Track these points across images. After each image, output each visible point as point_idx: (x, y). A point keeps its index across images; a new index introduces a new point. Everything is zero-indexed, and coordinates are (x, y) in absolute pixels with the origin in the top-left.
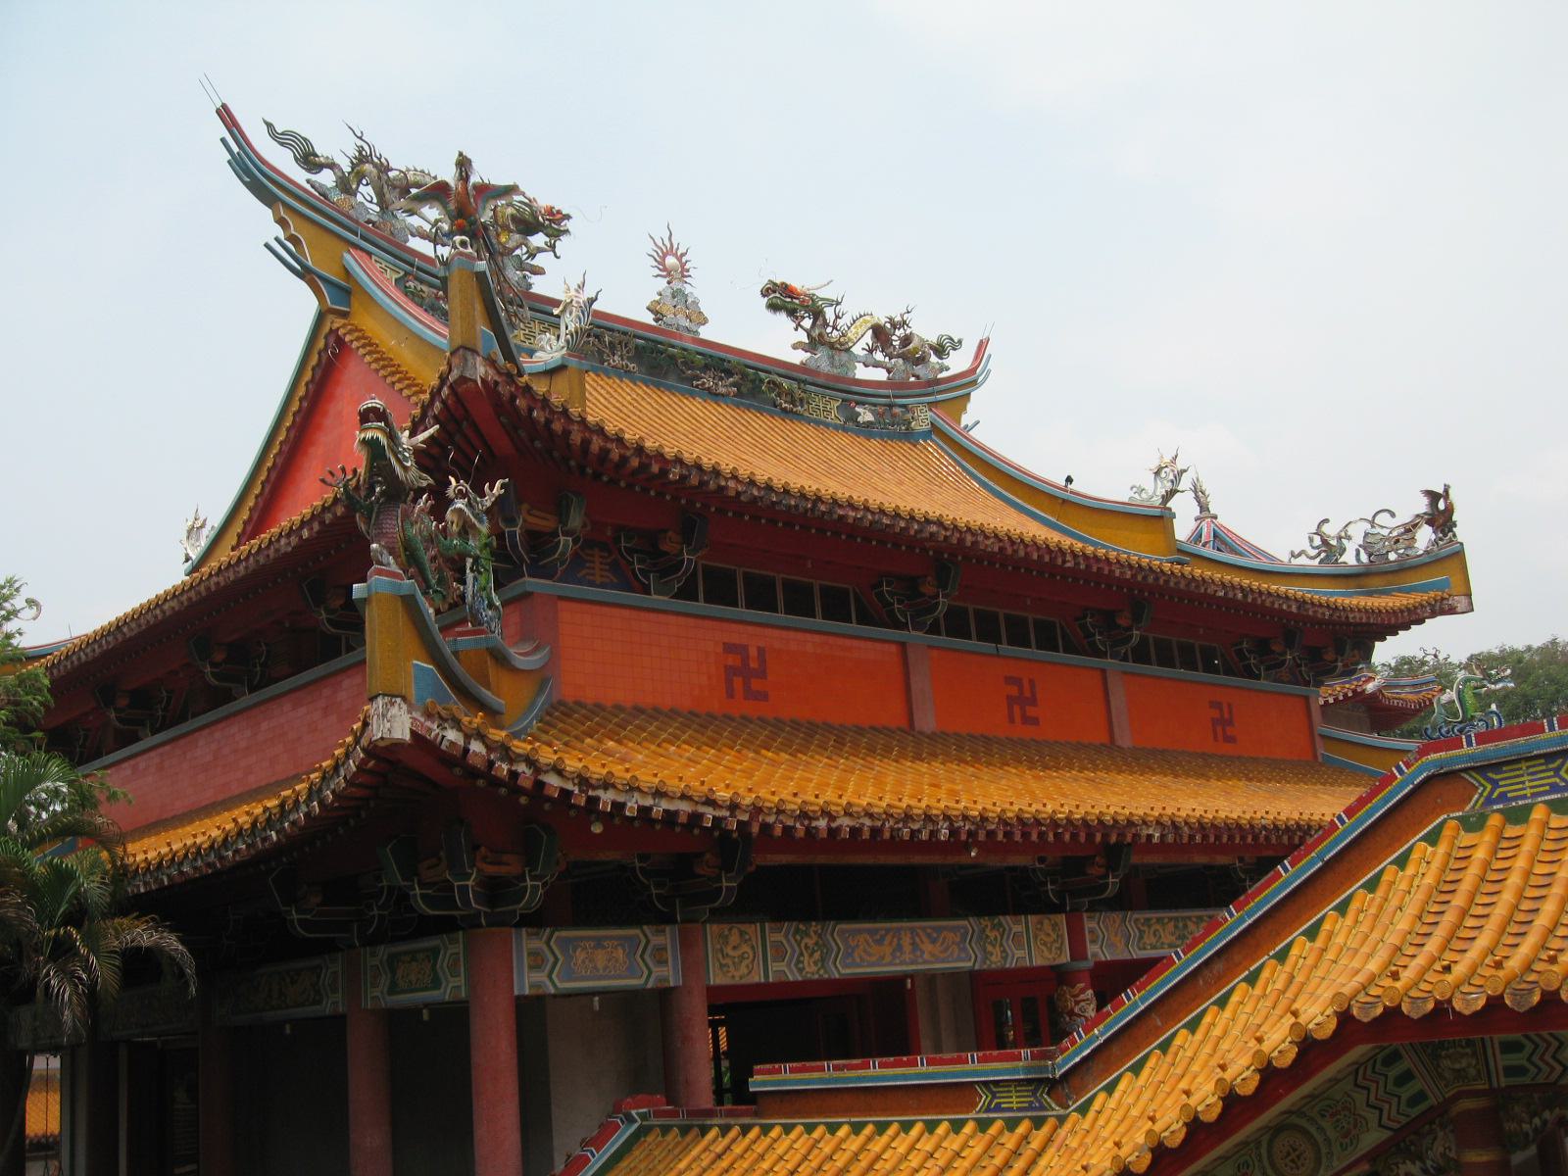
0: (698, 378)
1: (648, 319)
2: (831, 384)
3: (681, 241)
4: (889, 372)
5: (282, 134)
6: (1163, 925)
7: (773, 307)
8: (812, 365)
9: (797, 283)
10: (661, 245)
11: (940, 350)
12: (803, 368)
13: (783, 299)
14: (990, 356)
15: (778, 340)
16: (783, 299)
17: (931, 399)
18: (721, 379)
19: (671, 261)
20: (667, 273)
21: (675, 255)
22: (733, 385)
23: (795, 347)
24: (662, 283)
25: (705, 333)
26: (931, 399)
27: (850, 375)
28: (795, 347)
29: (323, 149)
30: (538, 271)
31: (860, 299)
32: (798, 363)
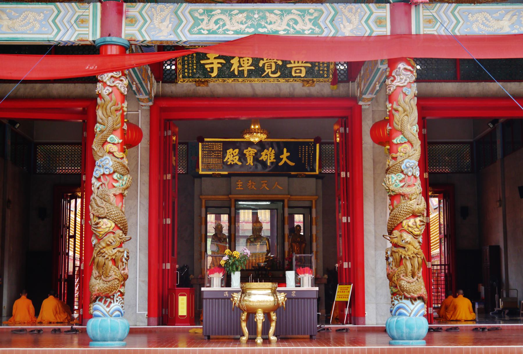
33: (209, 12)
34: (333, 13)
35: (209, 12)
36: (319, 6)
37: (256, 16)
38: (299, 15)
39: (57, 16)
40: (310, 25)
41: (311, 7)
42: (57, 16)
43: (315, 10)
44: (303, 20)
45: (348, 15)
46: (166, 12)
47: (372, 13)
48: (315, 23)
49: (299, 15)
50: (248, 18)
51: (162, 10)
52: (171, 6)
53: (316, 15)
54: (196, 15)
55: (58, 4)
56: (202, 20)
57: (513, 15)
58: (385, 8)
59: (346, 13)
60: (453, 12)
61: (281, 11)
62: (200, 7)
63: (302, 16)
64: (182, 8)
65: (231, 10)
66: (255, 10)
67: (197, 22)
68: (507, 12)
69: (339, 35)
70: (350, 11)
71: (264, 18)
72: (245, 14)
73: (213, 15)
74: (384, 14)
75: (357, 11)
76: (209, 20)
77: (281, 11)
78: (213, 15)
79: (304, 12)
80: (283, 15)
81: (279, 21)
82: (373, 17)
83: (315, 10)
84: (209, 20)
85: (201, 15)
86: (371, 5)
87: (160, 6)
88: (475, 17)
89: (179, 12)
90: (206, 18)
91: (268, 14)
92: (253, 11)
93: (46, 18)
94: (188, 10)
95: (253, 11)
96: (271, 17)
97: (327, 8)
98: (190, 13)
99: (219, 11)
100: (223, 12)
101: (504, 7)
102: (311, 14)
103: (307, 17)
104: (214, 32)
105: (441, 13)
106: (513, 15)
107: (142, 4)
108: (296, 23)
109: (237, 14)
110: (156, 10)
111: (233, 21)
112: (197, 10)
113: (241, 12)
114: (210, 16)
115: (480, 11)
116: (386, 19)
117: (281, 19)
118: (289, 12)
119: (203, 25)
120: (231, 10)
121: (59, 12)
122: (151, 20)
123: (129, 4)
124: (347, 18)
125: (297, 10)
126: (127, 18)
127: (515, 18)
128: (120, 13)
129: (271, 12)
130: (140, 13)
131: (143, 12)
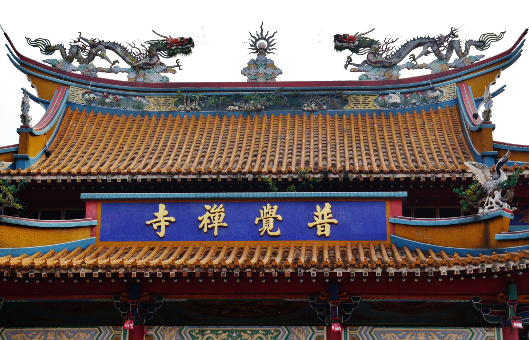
1: (244, 79)
3: (269, 30)
4: (432, 69)
5: (35, 41)
6: (217, 335)
8: (365, 79)
9: (352, 33)
11: (481, 45)
12: (359, 82)
14: (525, 40)
17: (459, 79)
20: (261, 51)
21: (264, 39)
24: (255, 56)
26: (459, 79)
27: (394, 78)
30: (170, 69)
31: (392, 30)
32: (358, 80)
33: (202, 332)
34: (287, 332)
35: (202, 332)
37: (235, 335)
38: (264, 334)
39: (99, 335)
41: (272, 329)
42: (99, 335)
43: (275, 331)
44: (267, 338)
46: (173, 332)
47: (314, 333)
49: (264, 334)
51: (170, 331)
53: (275, 334)
54: (194, 334)
55: (101, 327)
56: (198, 338)
57: (412, 335)
58: (323, 329)
59: (296, 333)
60: (370, 333)
61: (252, 331)
62: (197, 329)
63: (266, 335)
64: (184, 329)
65: (218, 331)
66: (234, 330)
68: (408, 333)
70: (299, 331)
72: (227, 334)
73: (205, 334)
74: (322, 334)
75: (303, 331)
76: (202, 338)
77: (252, 331)
78: (205, 334)
79: (267, 333)
80: (253, 334)
81: (250, 338)
82: (315, 336)
83: (275, 331)
84: (202, 338)
85: (197, 334)
86: (313, 327)
87: (169, 328)
88: (386, 336)
89: (182, 332)
90: (200, 336)
91: (242, 334)
92: (232, 332)
93: (92, 337)
94: (188, 331)
95: (232, 332)
97: (283, 330)
98: (190, 333)
99: (209, 332)
100: (212, 332)
101: (406, 329)
102: (272, 334)
103: (269, 336)
105: (362, 333)
106: (412, 335)
107: (157, 327)
109: (221, 334)
110: (166, 331)
111: (219, 338)
112: (194, 331)
113: (224, 332)
114: (203, 335)
115: (389, 332)
116: (323, 337)
117: (252, 337)
118: (257, 332)
120: (218, 331)
121: (101, 332)
122: (163, 338)
123: (148, 327)
124: (297, 337)
125: (263, 331)
126: (146, 336)
127: (414, 337)
128: (142, 333)
129: (245, 332)
130: (156, 332)
131: (158, 332)
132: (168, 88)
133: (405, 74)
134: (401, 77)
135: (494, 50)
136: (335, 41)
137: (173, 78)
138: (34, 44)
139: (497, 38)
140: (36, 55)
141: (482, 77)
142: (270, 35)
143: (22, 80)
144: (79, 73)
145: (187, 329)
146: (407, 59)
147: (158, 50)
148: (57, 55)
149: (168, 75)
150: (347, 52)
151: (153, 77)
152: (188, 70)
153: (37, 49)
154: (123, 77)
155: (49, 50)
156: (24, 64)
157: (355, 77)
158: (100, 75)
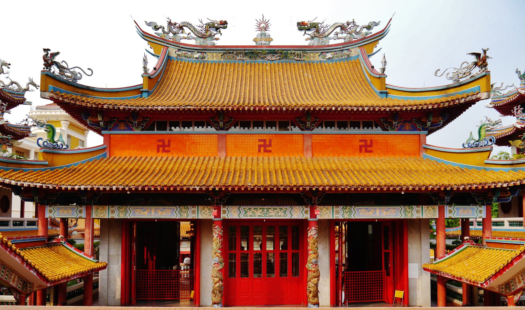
0: (266, 57)
1: (254, 44)
2: (317, 49)
7: (300, 29)
8: (311, 44)
9: (306, 21)
10: (259, 21)
11: (369, 28)
13: (302, 26)
15: (301, 39)
16: (302, 26)
18: (273, 56)
19: (262, 25)
20: (260, 29)
22: (279, 56)
23: (307, 40)
25: (272, 44)
28: (307, 40)
29: (159, 25)
30: (217, 39)
36: (286, 207)
40: (283, 213)
41: (284, 208)
45: (296, 210)
48: (285, 212)
50: (263, 211)
52: (238, 207)
67: (246, 212)
69: (293, 218)
71: (268, 211)
87: (234, 207)
96: (270, 211)
100: (254, 209)
103: (282, 211)
104: (252, 216)
108: (279, 213)
113: (260, 209)
118: (276, 209)
119: (248, 213)
129: (270, 209)
132: (215, 49)
133: (332, 42)
134: (330, 44)
135: (375, 30)
136: (298, 25)
137: (218, 43)
138: (149, 24)
139: (376, 24)
140: (150, 31)
141: (368, 45)
142: (267, 21)
143: (145, 44)
144: (171, 40)
145: (242, 208)
146: (332, 35)
147: (210, 27)
148: (160, 31)
149: (215, 41)
150: (303, 32)
151: (209, 42)
152: (225, 39)
153: (151, 28)
154: (193, 42)
155: (156, 28)
156: (145, 35)
157: (307, 43)
158: (182, 41)
